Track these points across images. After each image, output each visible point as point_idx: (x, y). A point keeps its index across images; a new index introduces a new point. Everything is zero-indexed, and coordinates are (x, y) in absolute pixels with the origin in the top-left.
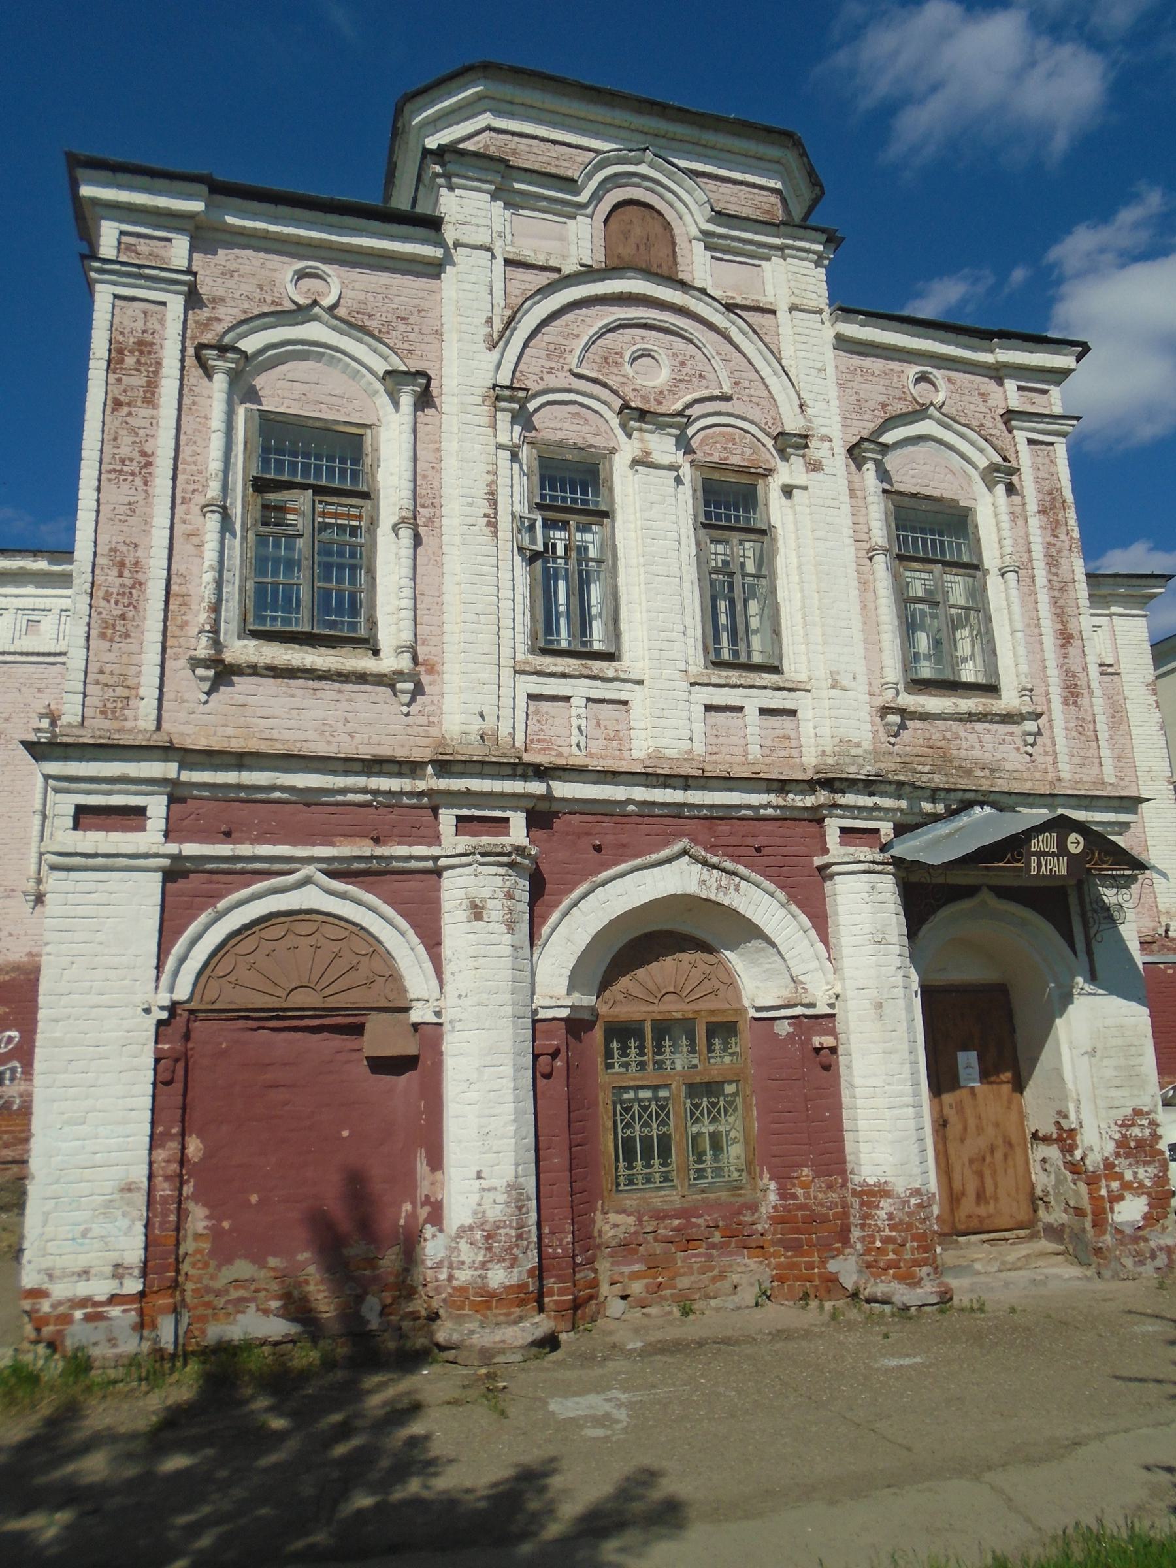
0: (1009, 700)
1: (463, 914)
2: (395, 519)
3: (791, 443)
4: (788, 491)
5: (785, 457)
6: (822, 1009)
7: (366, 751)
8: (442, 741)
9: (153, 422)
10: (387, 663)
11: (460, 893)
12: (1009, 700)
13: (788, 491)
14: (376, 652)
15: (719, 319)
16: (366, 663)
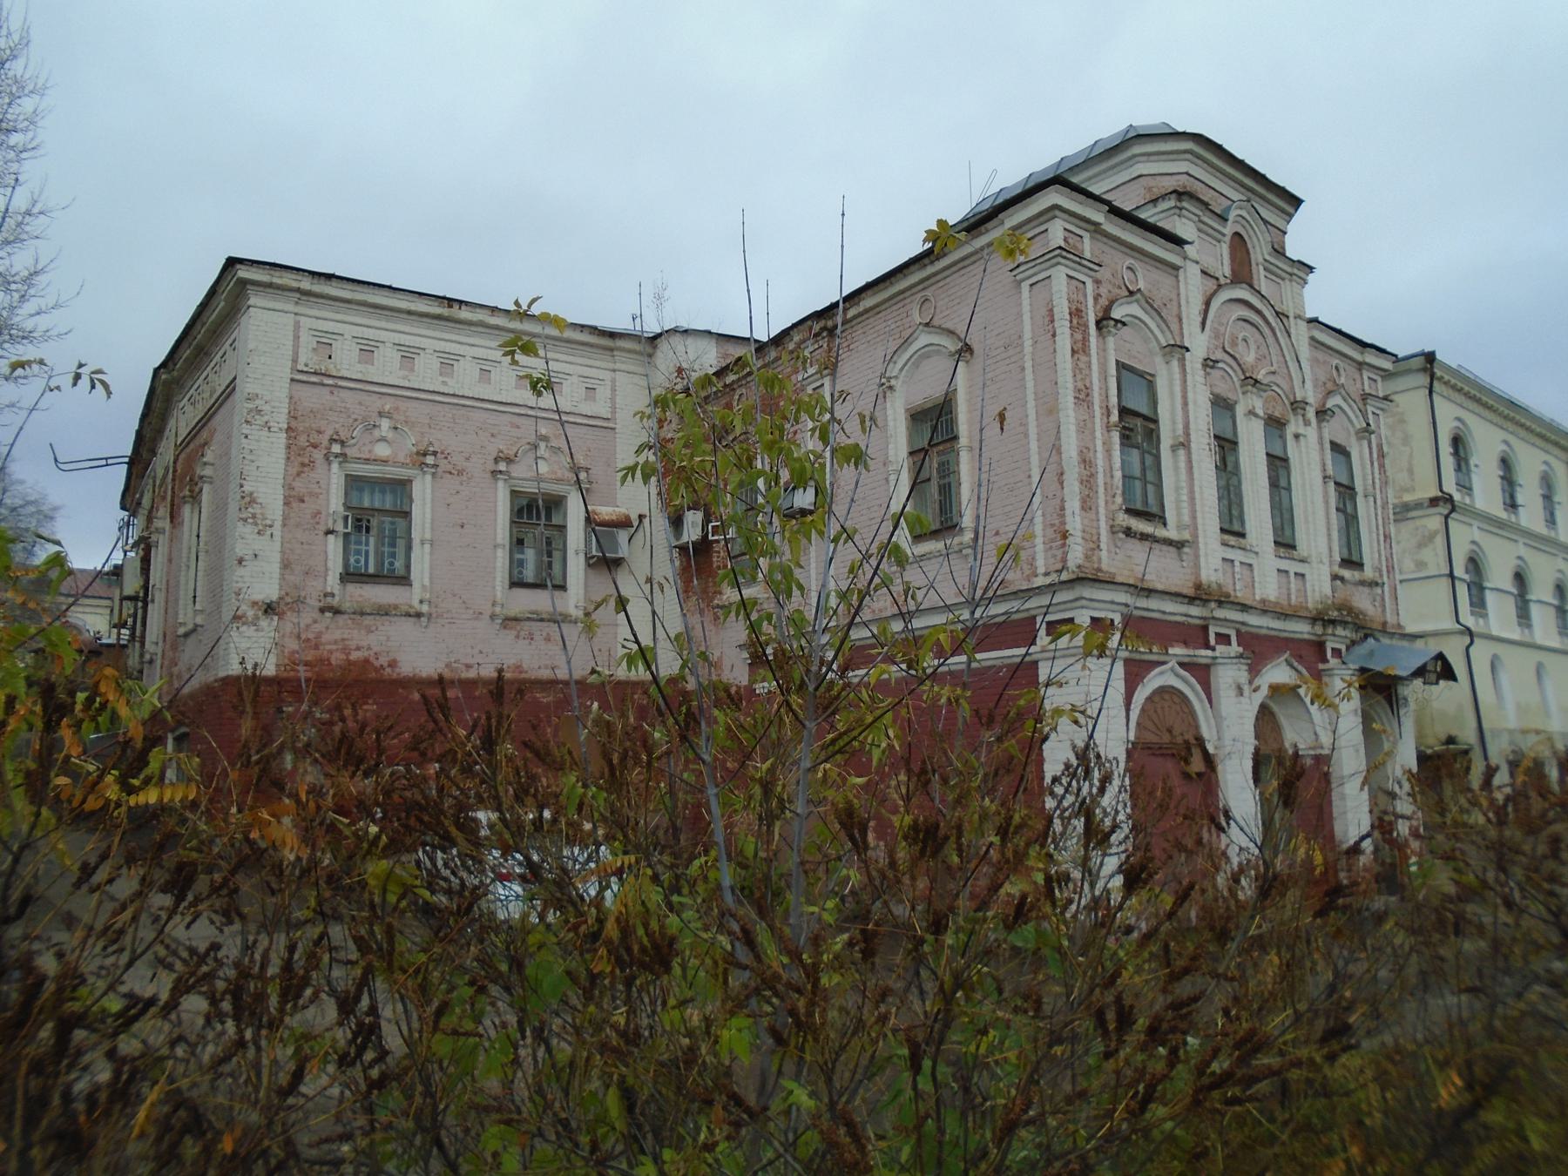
0: (1369, 573)
1: (1233, 693)
2: (1170, 442)
3: (1298, 406)
4: (1297, 436)
5: (1296, 414)
6: (1326, 752)
7: (1174, 589)
8: (1198, 586)
9: (1089, 363)
10: (1171, 533)
11: (1230, 680)
12: (1369, 573)
13: (1297, 436)
14: (1165, 524)
15: (1271, 319)
16: (1161, 532)
